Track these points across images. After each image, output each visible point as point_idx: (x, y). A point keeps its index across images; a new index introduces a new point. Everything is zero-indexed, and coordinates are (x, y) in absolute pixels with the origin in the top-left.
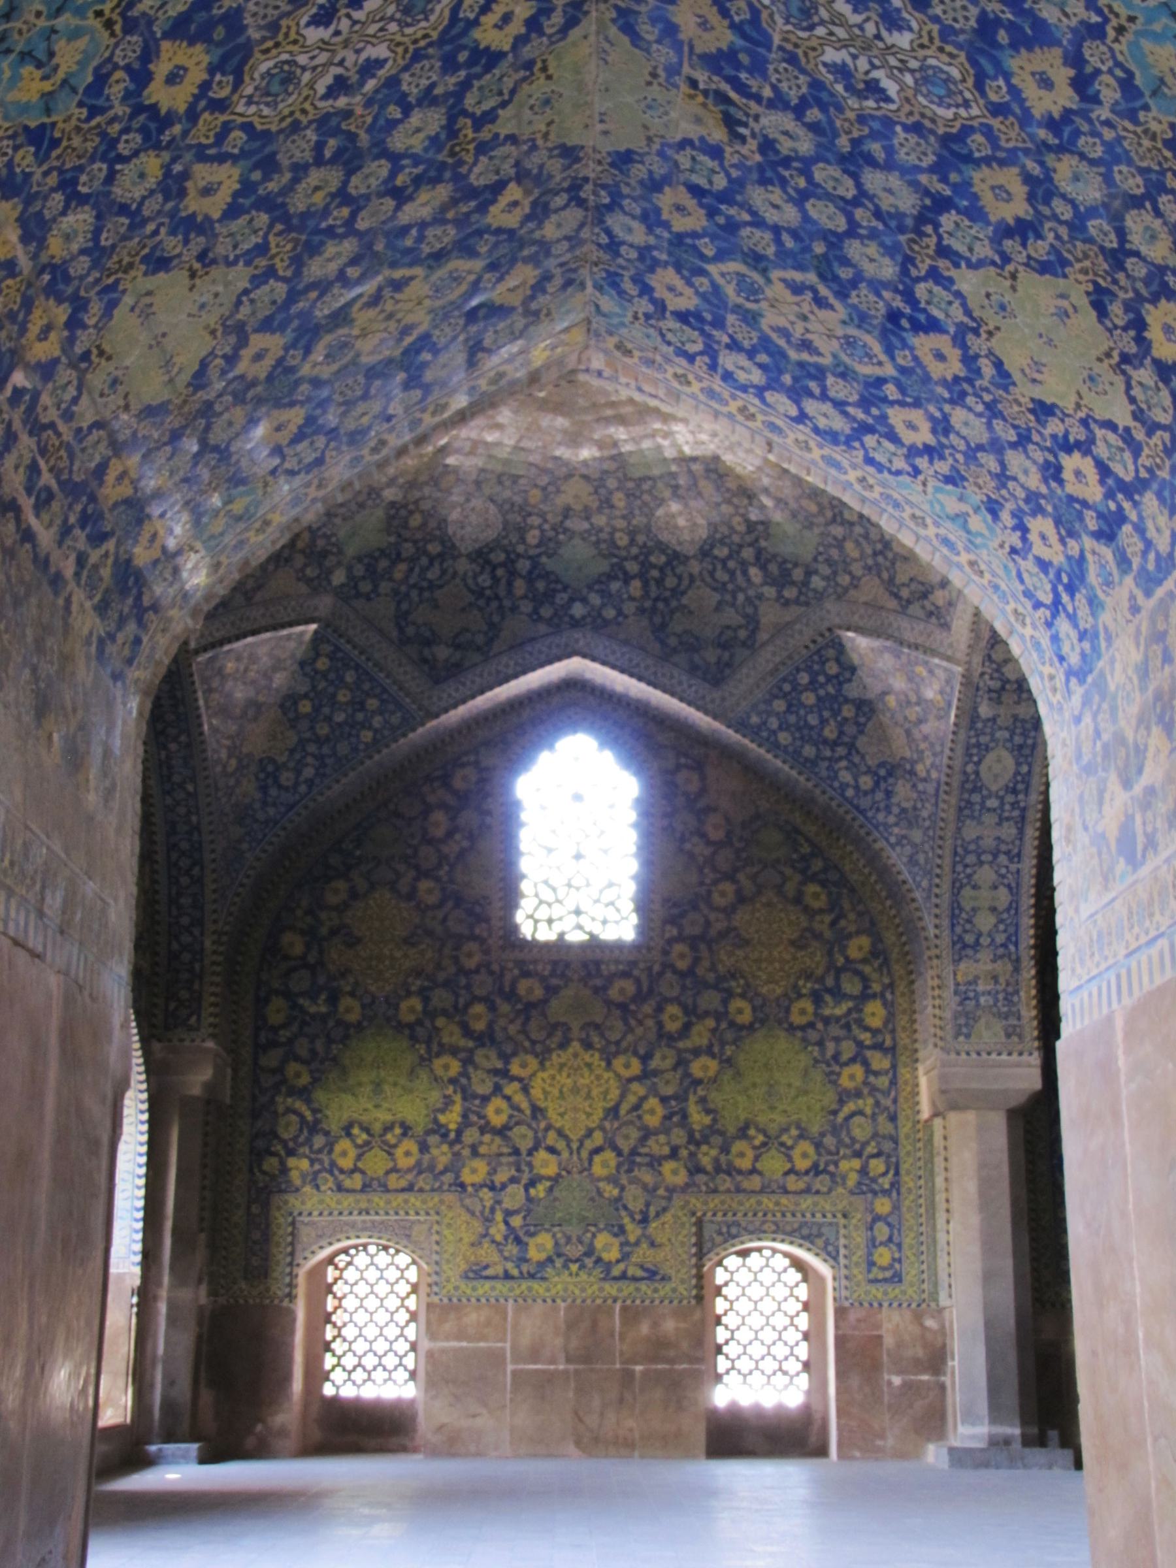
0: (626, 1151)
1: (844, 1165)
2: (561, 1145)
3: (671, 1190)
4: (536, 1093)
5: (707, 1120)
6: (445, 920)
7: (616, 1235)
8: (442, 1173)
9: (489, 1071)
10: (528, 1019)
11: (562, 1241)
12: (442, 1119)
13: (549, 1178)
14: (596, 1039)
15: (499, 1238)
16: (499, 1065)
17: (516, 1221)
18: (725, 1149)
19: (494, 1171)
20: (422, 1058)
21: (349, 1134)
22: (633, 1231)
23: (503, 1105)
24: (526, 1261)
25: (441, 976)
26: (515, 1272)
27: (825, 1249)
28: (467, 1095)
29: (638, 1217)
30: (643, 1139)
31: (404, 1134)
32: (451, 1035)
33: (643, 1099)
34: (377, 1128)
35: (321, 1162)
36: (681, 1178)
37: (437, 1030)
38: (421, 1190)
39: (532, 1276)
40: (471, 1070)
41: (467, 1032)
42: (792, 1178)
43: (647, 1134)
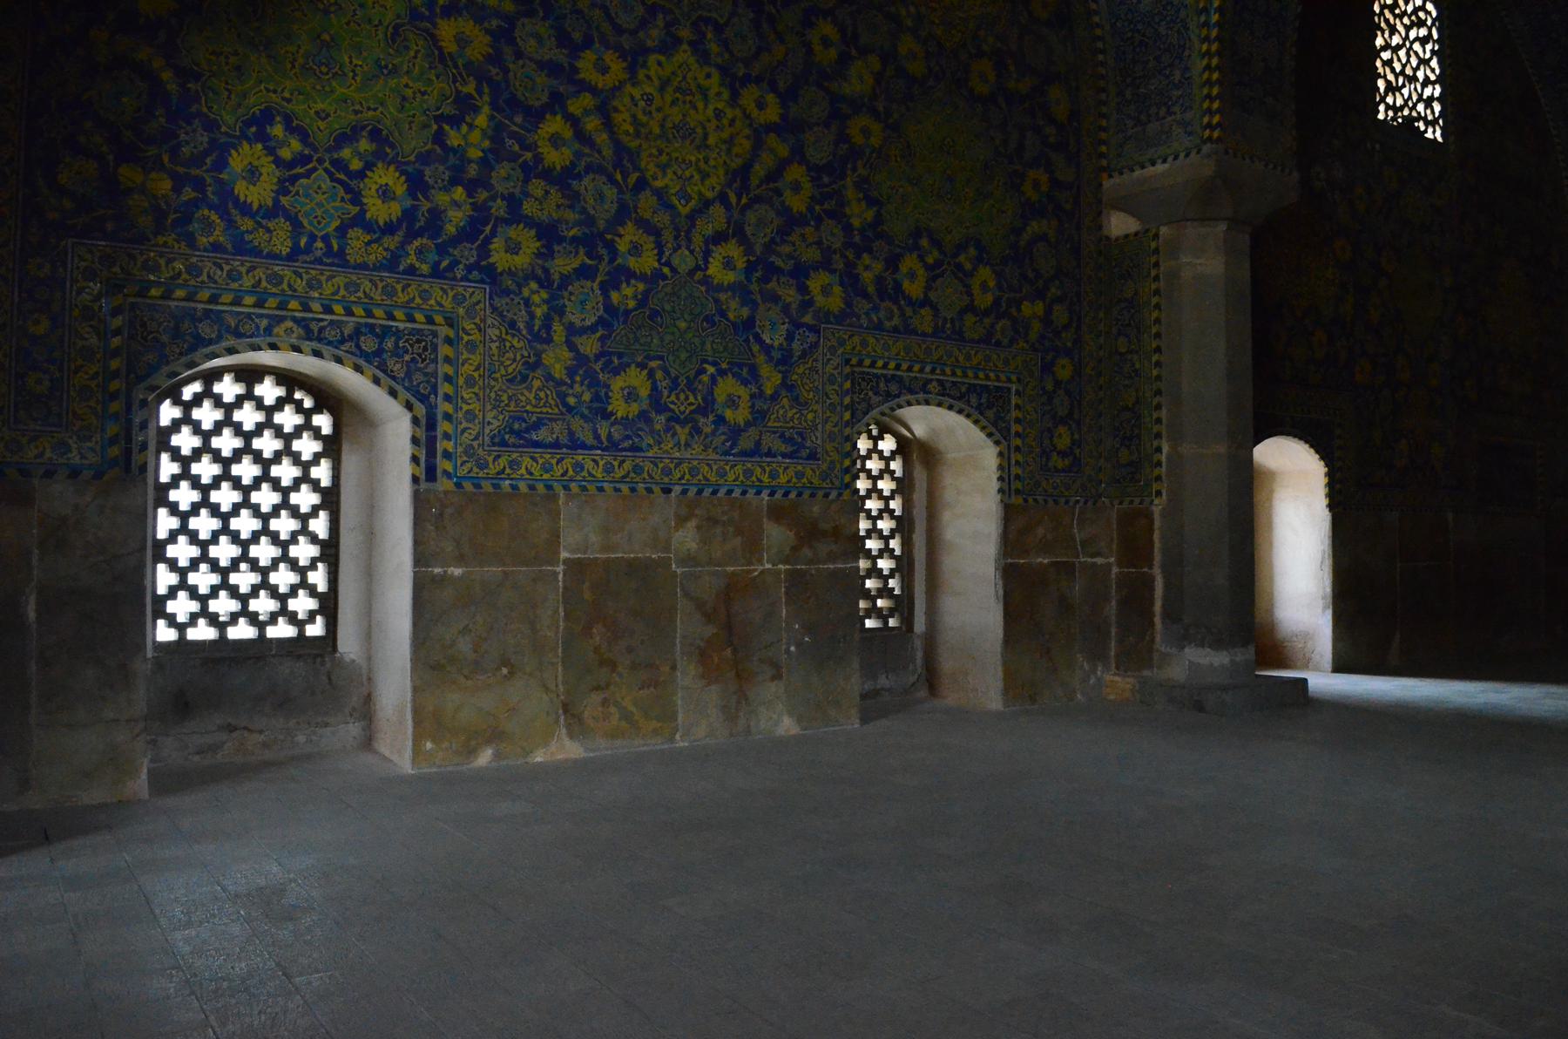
0: (758, 249)
1: (1027, 309)
2: (662, 219)
3: (826, 316)
4: (622, 120)
5: (870, 215)
7: (745, 383)
8: (456, 240)
9: (541, 65)
11: (663, 384)
12: (454, 138)
13: (642, 277)
14: (714, 48)
15: (559, 371)
16: (560, 56)
17: (589, 345)
18: (893, 263)
19: (546, 253)
21: (262, 137)
22: (771, 379)
23: (568, 133)
24: (607, 415)
26: (589, 439)
27: (995, 424)
28: (507, 103)
29: (776, 355)
30: (784, 232)
31: (379, 155)
33: (783, 165)
34: (322, 132)
35: (199, 185)
36: (835, 302)
39: (613, 446)
40: (508, 51)
42: (970, 319)
43: (792, 221)
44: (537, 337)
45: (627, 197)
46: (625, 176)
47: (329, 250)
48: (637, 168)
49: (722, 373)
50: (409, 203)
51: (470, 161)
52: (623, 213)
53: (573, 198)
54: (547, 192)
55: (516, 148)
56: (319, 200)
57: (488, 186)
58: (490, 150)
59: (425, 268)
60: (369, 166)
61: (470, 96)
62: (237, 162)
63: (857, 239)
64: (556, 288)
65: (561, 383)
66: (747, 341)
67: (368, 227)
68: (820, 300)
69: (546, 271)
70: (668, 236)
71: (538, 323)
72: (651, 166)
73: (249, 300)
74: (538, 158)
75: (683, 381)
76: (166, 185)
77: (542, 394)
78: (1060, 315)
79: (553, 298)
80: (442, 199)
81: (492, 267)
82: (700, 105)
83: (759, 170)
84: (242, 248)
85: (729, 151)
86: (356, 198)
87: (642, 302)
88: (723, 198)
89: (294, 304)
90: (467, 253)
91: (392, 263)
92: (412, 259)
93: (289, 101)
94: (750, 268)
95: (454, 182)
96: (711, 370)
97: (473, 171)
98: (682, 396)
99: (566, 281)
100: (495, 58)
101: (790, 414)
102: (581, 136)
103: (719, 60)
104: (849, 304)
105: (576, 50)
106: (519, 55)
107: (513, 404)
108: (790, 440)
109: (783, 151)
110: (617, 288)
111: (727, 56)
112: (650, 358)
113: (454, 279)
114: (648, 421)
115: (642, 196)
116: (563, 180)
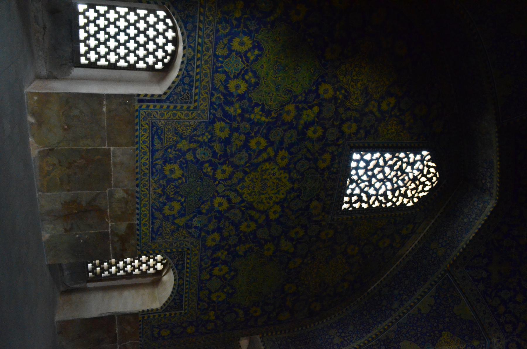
0: (227, 214)
2: (235, 180)
3: (204, 240)
4: (267, 165)
5: (241, 253)
6: (372, 112)
7: (179, 212)
8: (223, 110)
9: (282, 138)
10: (309, 160)
12: (257, 110)
13: (214, 174)
14: (292, 195)
15: (180, 146)
16: (286, 145)
17: (189, 156)
18: (225, 263)
19: (221, 141)
20: (296, 97)
21: (254, 47)
22: (181, 221)
23: (261, 148)
24: (164, 163)
25: (341, 110)
27: (168, 306)
28: (270, 127)
29: (189, 223)
30: (233, 223)
31: (250, 85)
32: (309, 115)
33: (256, 221)
34: (257, 67)
35: (238, 26)
36: (210, 243)
37: (311, 108)
38: (212, 95)
39: (153, 165)
40: (286, 127)
41: (307, 125)
42: (206, 292)
43: (237, 225)
44: (191, 138)
45: (241, 168)
46: (248, 167)
47: (218, 68)
48: (251, 171)
49: (182, 204)
50: (235, 94)
51: (250, 115)
52: (236, 167)
53: (240, 150)
54: (241, 141)
55: (255, 130)
56: (235, 65)
57: (242, 121)
58: (254, 122)
59: (214, 100)
60: (246, 82)
61: (271, 115)
62: (246, 39)
63: (232, 249)
64: (209, 144)
65: (175, 146)
66: (194, 212)
67: (227, 81)
68: (210, 238)
69: (214, 141)
70: (229, 183)
71: (196, 138)
72: (252, 176)
73: (200, 40)
74: (252, 138)
75: (178, 190)
76: (237, 15)
77: (171, 140)
78: (210, 326)
79: (205, 143)
80: (237, 105)
81: (215, 123)
82: (273, 192)
83: (253, 213)
84: (218, 39)
85: (259, 202)
86: (236, 77)
87: (205, 174)
88: (243, 201)
89: (199, 55)
90: (219, 114)
91: (214, 88)
92: (216, 95)
93: (266, 56)
94: (219, 212)
95: (243, 110)
96: (183, 200)
97: (247, 116)
98: (172, 190)
99: (211, 148)
100: (284, 123)
101: (168, 229)
102: (260, 152)
103: (288, 197)
104: (209, 248)
105: (288, 149)
106: (285, 131)
107: (167, 130)
108: (158, 230)
109: (260, 221)
110: (210, 166)
111: (290, 200)
112: (186, 178)
113: (210, 109)
114: (163, 179)
115: (242, 173)
116: (246, 146)
